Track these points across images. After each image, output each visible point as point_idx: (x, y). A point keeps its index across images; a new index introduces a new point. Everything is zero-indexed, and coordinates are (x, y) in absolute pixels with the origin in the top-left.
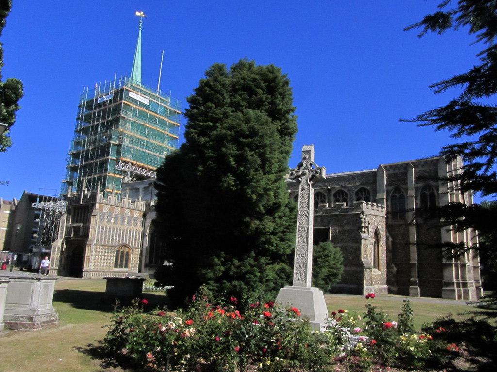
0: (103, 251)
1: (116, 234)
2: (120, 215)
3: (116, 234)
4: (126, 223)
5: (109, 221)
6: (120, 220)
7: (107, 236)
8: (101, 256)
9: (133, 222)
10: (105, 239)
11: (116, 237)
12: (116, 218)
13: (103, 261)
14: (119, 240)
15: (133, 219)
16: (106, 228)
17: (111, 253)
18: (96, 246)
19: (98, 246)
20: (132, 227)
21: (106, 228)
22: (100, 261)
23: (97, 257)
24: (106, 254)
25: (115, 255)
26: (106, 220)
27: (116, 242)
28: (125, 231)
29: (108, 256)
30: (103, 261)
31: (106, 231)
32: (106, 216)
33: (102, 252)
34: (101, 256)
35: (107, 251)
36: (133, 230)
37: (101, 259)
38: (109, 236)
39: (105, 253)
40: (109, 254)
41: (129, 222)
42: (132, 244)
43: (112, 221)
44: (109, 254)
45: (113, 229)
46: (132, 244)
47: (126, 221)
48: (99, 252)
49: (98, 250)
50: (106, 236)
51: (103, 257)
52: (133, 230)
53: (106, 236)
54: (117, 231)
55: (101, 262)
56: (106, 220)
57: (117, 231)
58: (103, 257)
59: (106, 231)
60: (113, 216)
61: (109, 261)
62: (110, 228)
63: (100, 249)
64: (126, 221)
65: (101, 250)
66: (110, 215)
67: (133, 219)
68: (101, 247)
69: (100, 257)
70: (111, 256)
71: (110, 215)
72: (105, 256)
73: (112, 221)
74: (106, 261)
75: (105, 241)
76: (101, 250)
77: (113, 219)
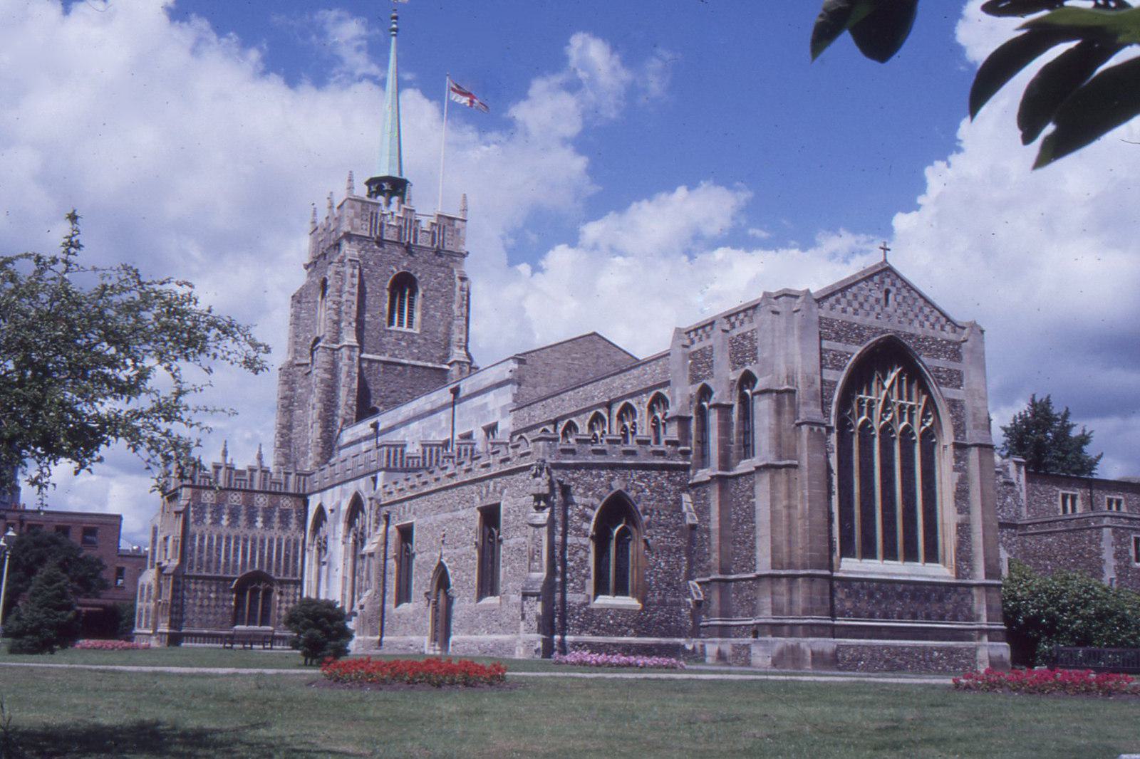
1: (236, 550)
2: (243, 507)
3: (236, 550)
4: (259, 524)
5: (216, 522)
6: (242, 520)
8: (202, 599)
11: (236, 555)
12: (234, 514)
14: (244, 562)
15: (277, 514)
16: (211, 539)
20: (275, 532)
21: (211, 539)
22: (197, 609)
24: (212, 595)
26: (208, 521)
28: (258, 541)
29: (217, 599)
31: (210, 546)
32: (209, 510)
33: (202, 591)
34: (202, 599)
35: (214, 588)
36: (279, 540)
37: (201, 606)
40: (221, 595)
41: (267, 521)
43: (225, 522)
44: (221, 595)
47: (260, 519)
48: (195, 591)
51: (206, 602)
52: (279, 540)
56: (208, 521)
57: (236, 543)
58: (206, 602)
59: (210, 546)
60: (227, 511)
63: (196, 583)
64: (260, 519)
65: (199, 587)
67: (277, 514)
70: (224, 600)
72: (209, 598)
73: (225, 522)
76: (199, 587)
77: (225, 517)
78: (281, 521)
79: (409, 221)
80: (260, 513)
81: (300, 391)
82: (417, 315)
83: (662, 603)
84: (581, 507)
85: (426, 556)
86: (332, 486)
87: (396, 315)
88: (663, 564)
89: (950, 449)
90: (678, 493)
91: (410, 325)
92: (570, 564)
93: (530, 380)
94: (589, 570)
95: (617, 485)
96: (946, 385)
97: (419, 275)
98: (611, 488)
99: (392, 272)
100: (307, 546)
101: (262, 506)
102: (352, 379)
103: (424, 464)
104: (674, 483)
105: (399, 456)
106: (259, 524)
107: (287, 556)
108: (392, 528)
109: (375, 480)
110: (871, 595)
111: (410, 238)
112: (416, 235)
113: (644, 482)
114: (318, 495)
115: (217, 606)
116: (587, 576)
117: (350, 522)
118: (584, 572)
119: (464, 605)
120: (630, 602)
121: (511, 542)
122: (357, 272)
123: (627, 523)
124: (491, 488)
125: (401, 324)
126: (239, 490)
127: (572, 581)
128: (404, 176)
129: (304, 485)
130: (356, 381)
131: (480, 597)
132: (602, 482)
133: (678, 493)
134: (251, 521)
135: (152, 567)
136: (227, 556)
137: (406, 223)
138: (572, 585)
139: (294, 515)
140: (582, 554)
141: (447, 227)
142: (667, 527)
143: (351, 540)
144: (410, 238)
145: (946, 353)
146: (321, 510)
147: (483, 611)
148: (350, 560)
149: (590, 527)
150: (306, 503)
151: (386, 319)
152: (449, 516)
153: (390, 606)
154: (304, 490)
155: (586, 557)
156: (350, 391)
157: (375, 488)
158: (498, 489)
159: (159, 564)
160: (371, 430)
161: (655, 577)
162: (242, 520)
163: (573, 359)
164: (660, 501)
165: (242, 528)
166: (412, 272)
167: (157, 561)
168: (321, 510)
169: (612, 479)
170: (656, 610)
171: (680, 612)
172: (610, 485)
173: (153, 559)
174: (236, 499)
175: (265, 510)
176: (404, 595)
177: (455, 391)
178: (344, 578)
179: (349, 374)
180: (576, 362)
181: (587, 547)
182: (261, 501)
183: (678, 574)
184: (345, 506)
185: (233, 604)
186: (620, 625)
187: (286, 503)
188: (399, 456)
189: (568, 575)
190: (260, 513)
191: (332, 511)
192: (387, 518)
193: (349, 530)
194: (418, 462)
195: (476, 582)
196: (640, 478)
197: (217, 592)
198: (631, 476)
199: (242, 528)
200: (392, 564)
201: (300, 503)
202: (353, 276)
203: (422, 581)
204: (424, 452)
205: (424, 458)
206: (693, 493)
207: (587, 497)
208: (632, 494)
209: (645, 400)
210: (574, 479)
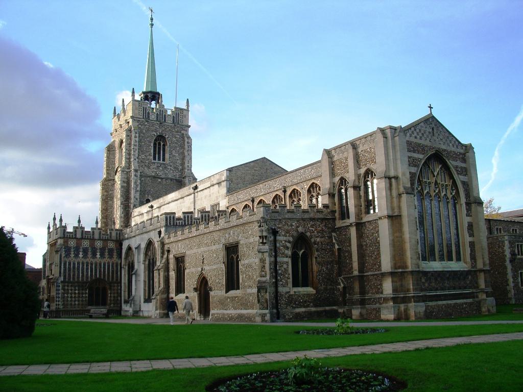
0: (73, 288)
1: (87, 269)
2: (90, 248)
3: (87, 269)
4: (98, 256)
5: (77, 255)
6: (90, 254)
7: (76, 272)
8: (71, 294)
9: (107, 254)
10: (74, 275)
12: (85, 251)
13: (73, 299)
14: (92, 275)
15: (107, 251)
16: (74, 264)
17: (82, 290)
18: (63, 284)
19: (66, 284)
20: (106, 259)
21: (74, 264)
23: (66, 295)
24: (77, 292)
25: (87, 292)
26: (72, 255)
27: (87, 277)
29: (79, 293)
30: (73, 299)
31: (74, 267)
32: (72, 250)
33: (71, 290)
34: (71, 294)
35: (77, 288)
36: (108, 263)
37: (71, 297)
38: (79, 272)
39: (75, 290)
40: (81, 292)
41: (102, 255)
42: (108, 278)
43: (81, 255)
44: (81, 292)
45: (83, 263)
46: (108, 278)
47: (98, 254)
48: (68, 290)
49: (66, 288)
50: (74, 271)
51: (73, 296)
52: (108, 263)
53: (74, 271)
54: (87, 265)
55: (71, 301)
56: (72, 255)
57: (87, 265)
58: (73, 296)
59: (74, 267)
60: (81, 250)
61: (81, 299)
62: (78, 263)
63: (68, 286)
64: (98, 254)
65: (70, 288)
66: (77, 249)
67: (107, 251)
68: (70, 285)
69: (69, 295)
70: (83, 294)
71: (77, 249)
72: (75, 293)
73: (81, 255)
74: (77, 299)
75: (74, 278)
76: (70, 288)
77: (81, 253)
78: (109, 254)
79: (162, 113)
80: (98, 251)
81: (110, 192)
82: (167, 156)
83: (326, 289)
84: (283, 242)
85: (193, 270)
86: (135, 236)
87: (157, 156)
88: (325, 269)
89: (464, 205)
90: (330, 233)
91: (164, 160)
92: (280, 272)
93: (235, 181)
94: (289, 275)
95: (300, 229)
96: (461, 174)
97: (167, 136)
98: (298, 232)
99: (154, 135)
100: (122, 266)
101: (99, 247)
102: (137, 186)
103: (185, 223)
104: (329, 228)
105: (172, 220)
106: (98, 256)
107: (113, 271)
108: (171, 256)
109: (160, 233)
110: (436, 279)
111: (162, 119)
112: (165, 118)
113: (313, 228)
114: (127, 241)
115: (79, 297)
116: (289, 278)
117: (146, 254)
118: (286, 276)
119: (217, 293)
120: (310, 290)
121: (246, 262)
122: (137, 135)
123: (306, 249)
124: (231, 234)
125: (159, 159)
126: (88, 239)
127: (281, 281)
128: (158, 91)
129: (120, 236)
130: (139, 186)
131: (227, 292)
132: (293, 229)
133: (330, 233)
134: (94, 255)
135: (44, 278)
136: (83, 273)
137: (160, 112)
138: (281, 283)
139: (115, 251)
140: (285, 266)
141: (180, 114)
142: (326, 251)
143: (147, 263)
144: (162, 119)
145: (459, 159)
146: (129, 248)
147: (228, 297)
148: (147, 272)
149: (289, 253)
150: (121, 245)
151: (152, 157)
152: (205, 249)
153: (172, 295)
154: (120, 238)
155: (288, 267)
156: (136, 191)
157: (160, 237)
158: (236, 234)
159: (48, 276)
160: (149, 209)
161: (322, 276)
162: (90, 254)
163: (255, 170)
164: (322, 237)
165: (90, 259)
166: (164, 135)
167: (46, 275)
168: (129, 248)
169: (298, 227)
170: (323, 293)
171: (334, 293)
172: (297, 230)
173: (45, 274)
174: (86, 244)
175: (100, 249)
176: (180, 289)
177: (196, 188)
178: (145, 282)
179: (135, 183)
180: (256, 172)
181: (287, 262)
182: (99, 244)
183: (332, 274)
184: (143, 246)
185: (87, 295)
186: (305, 302)
187: (111, 245)
188: (172, 220)
189: (279, 278)
190: (98, 251)
191: (136, 248)
192: (169, 251)
193: (145, 257)
194: (182, 223)
195: (224, 283)
196: (312, 226)
197: (79, 290)
198: (307, 225)
199: (90, 259)
200: (172, 274)
201: (118, 245)
202: (135, 137)
203: (191, 282)
204: (185, 217)
205: (185, 221)
206: (338, 232)
207: (286, 236)
208: (308, 234)
209: (306, 187)
210: (279, 228)
